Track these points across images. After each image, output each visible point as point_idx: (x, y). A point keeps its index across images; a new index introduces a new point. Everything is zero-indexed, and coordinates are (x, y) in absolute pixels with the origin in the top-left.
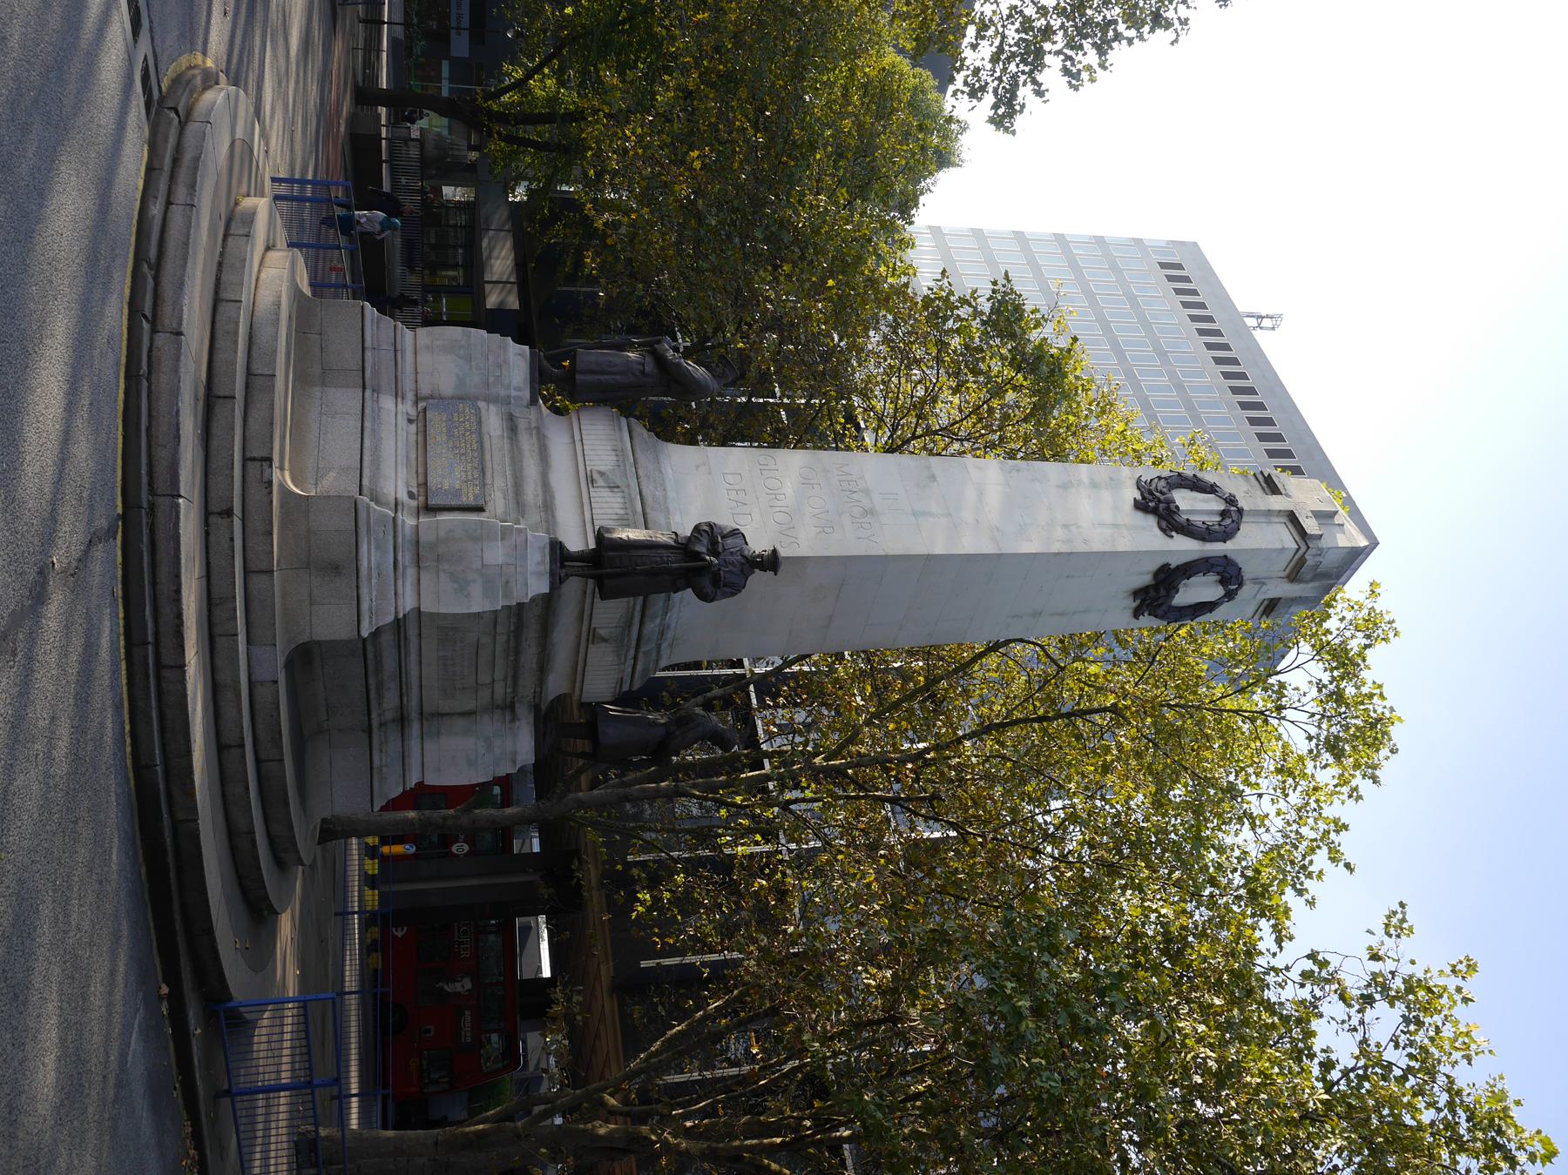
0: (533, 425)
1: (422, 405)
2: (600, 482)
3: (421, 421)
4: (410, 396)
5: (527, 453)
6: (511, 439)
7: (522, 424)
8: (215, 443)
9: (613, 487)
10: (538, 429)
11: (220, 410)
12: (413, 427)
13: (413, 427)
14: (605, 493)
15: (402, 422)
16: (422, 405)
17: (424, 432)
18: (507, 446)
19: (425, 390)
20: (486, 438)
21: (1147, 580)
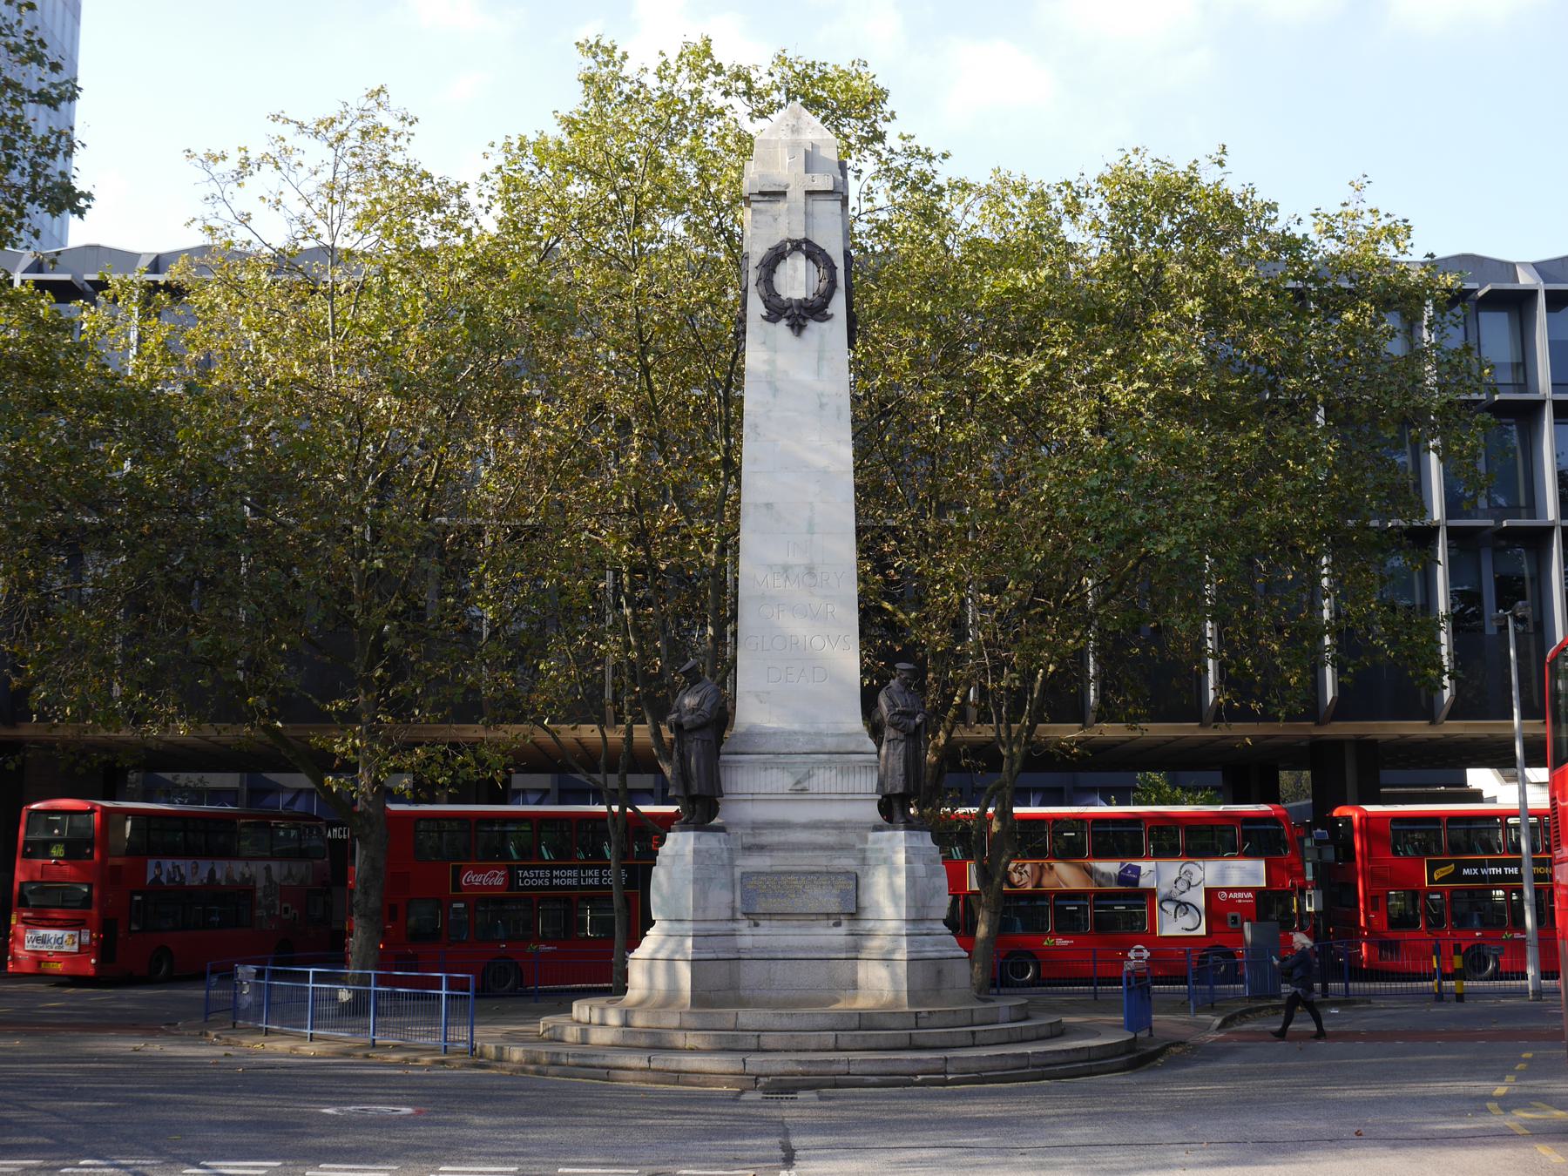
1: (739, 916)
2: (805, 784)
3: (754, 917)
4: (735, 925)
5: (782, 839)
6: (772, 850)
7: (749, 840)
8: (938, 1044)
9: (809, 776)
11: (920, 1041)
12: (762, 923)
13: (762, 923)
14: (814, 780)
15: (756, 931)
16: (739, 916)
17: (770, 915)
18: (781, 854)
19: (727, 914)
20: (775, 869)
21: (812, 325)
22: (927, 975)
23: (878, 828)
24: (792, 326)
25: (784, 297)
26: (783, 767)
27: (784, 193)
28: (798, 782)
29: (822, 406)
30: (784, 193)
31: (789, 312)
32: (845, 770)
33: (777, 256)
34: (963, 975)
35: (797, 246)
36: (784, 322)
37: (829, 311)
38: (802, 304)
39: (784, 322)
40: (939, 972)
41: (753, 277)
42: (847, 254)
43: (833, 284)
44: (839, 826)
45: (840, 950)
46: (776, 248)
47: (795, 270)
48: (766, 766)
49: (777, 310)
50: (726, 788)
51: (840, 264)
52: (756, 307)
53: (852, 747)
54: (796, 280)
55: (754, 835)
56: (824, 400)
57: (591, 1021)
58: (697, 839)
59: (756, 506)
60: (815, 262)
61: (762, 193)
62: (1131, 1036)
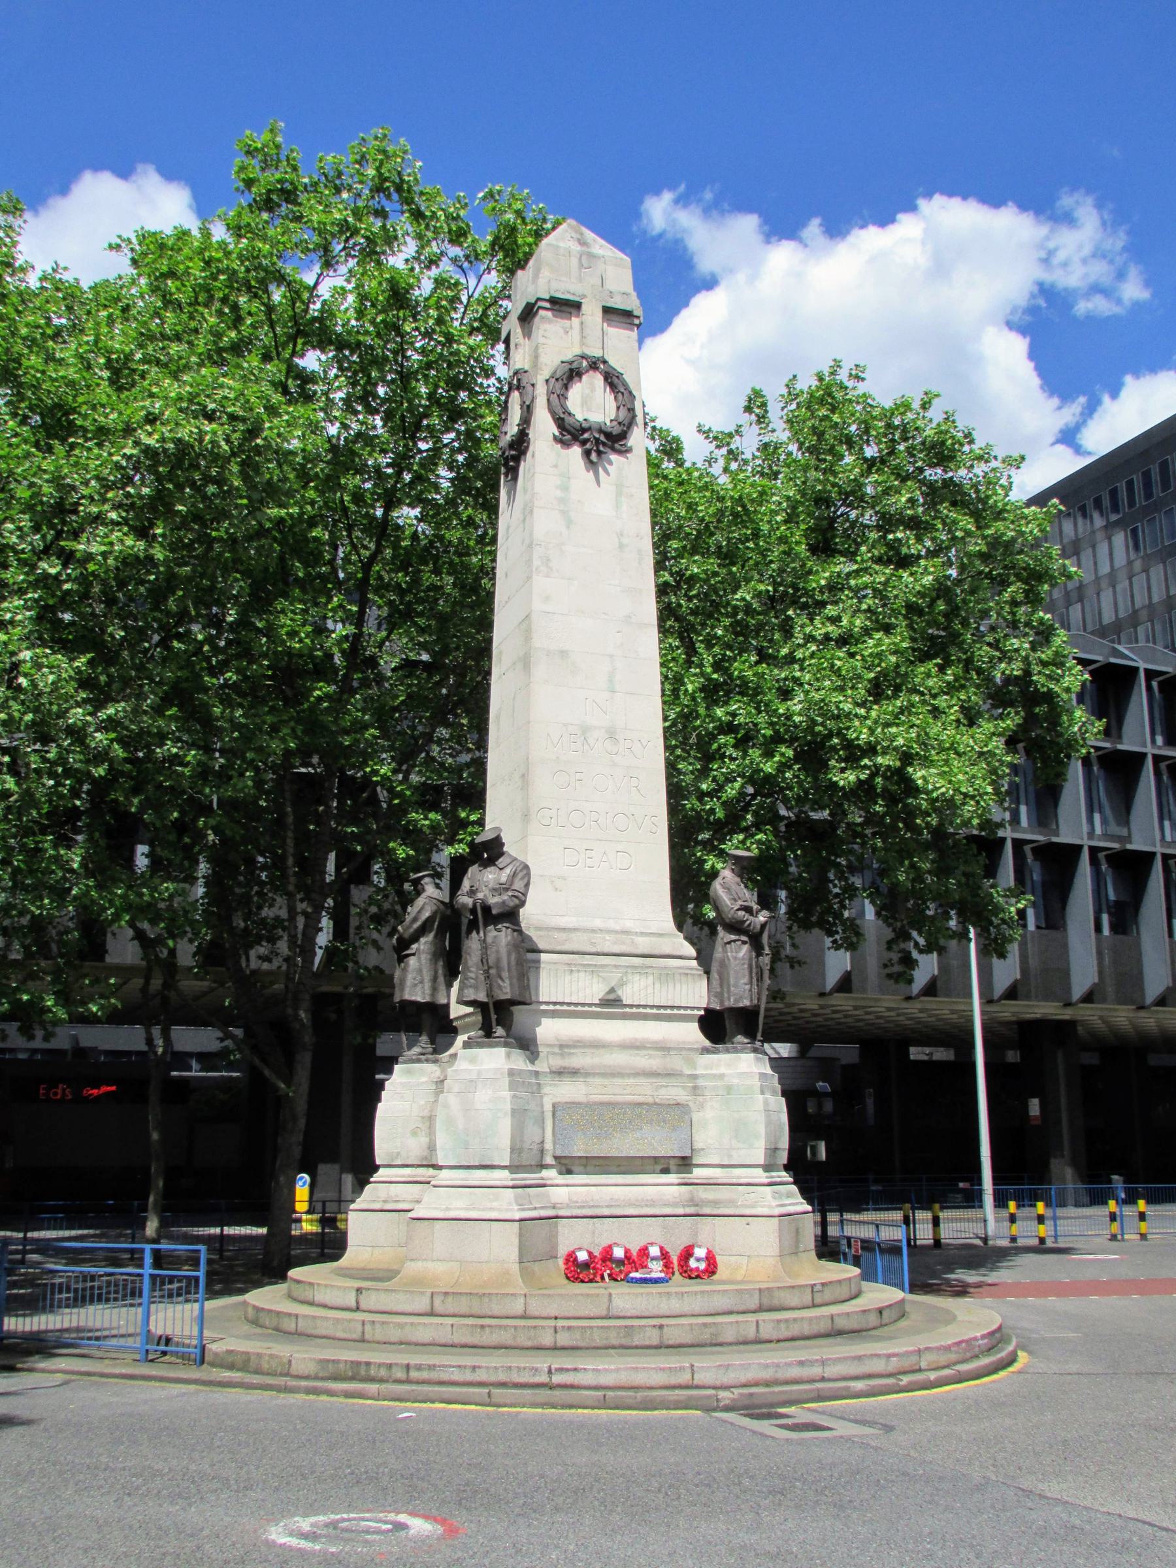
0: (557, 1050)
6: (587, 1075)
10: (561, 1046)
23: (705, 1051)
24: (587, 453)
25: (580, 417)
26: (593, 970)
28: (612, 990)
29: (621, 546)
31: (586, 436)
32: (666, 976)
33: (572, 374)
35: (594, 365)
36: (576, 450)
39: (576, 450)
44: (663, 1048)
47: (593, 390)
48: (571, 968)
49: (571, 432)
52: (543, 427)
53: (667, 950)
55: (562, 1055)
56: (625, 541)
58: (508, 1055)
61: (554, 301)
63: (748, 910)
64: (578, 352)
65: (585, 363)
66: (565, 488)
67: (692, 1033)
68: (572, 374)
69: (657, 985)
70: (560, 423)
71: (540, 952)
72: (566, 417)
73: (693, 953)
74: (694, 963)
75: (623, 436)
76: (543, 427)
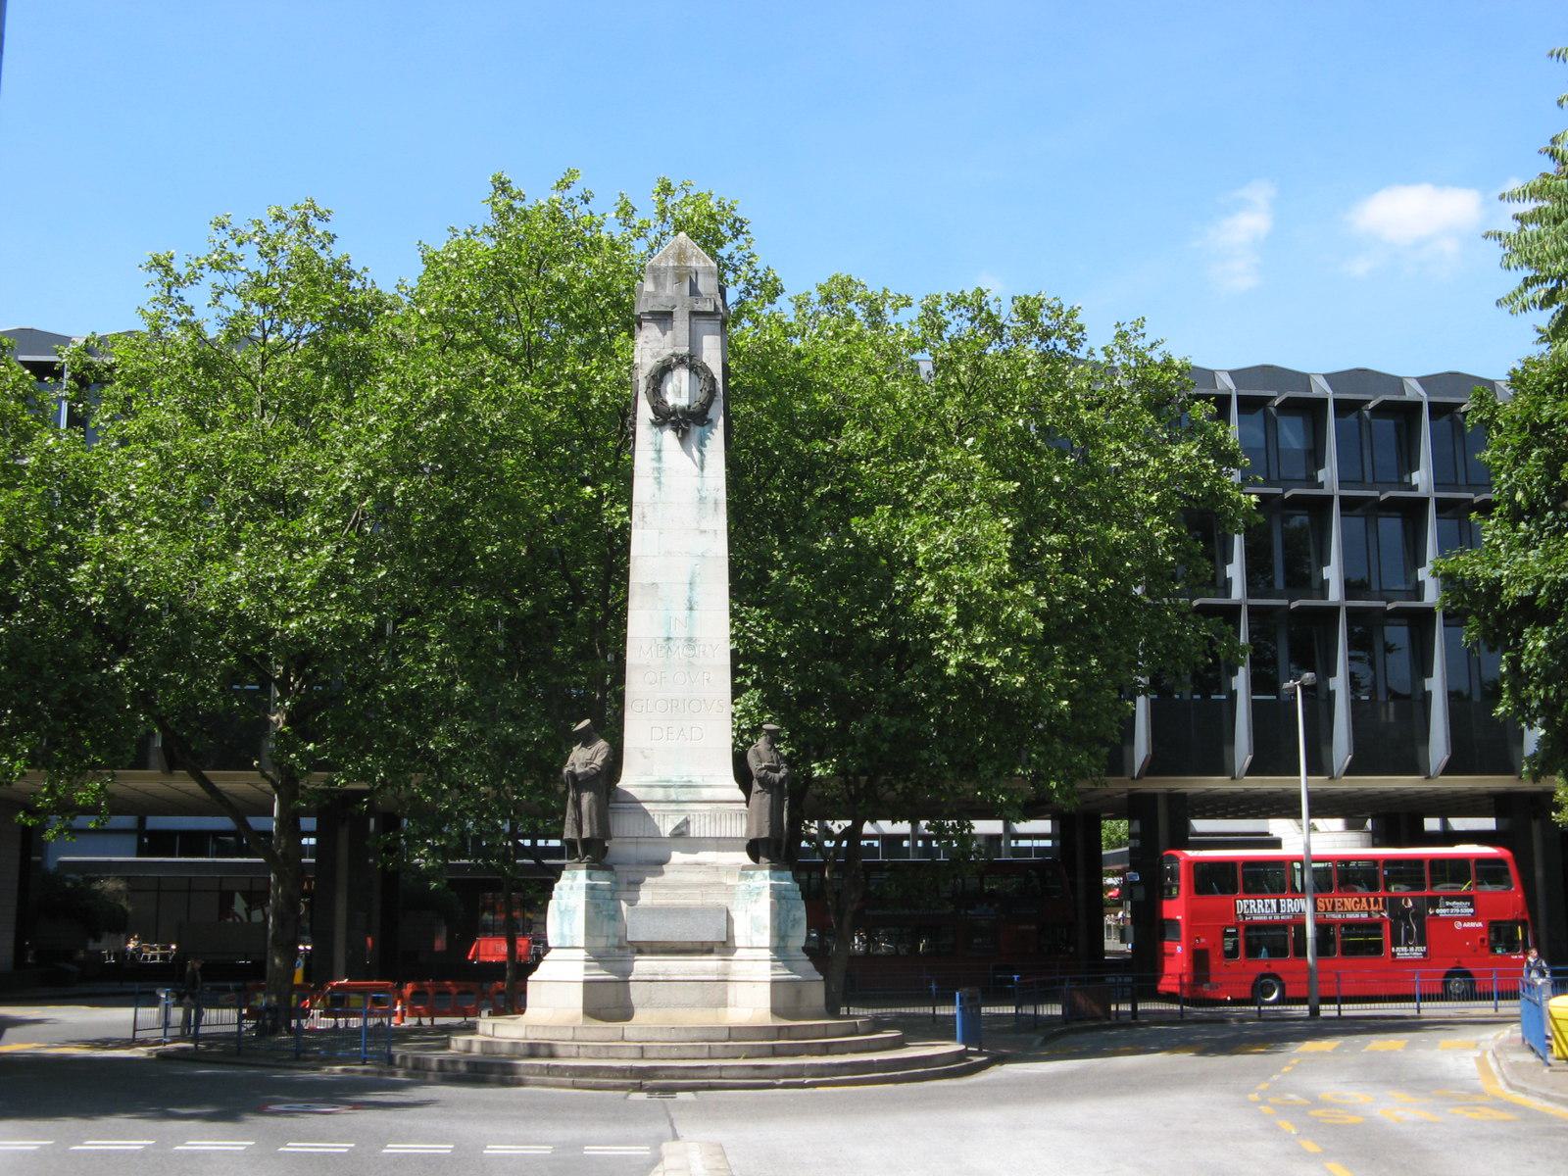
22: (785, 997)
27: (670, 314)
30: (670, 314)
33: (663, 371)
34: (817, 994)
35: (681, 361)
37: (709, 417)
38: (683, 411)
40: (799, 992)
41: (642, 385)
42: (725, 368)
43: (712, 394)
45: (712, 973)
46: (664, 361)
49: (664, 417)
50: (615, 831)
51: (719, 377)
52: (644, 411)
54: (679, 391)
57: (497, 1031)
59: (643, 586)
60: (696, 373)
62: (963, 1047)
63: (768, 768)
64: (671, 352)
65: (674, 360)
66: (659, 459)
67: (744, 858)
68: (663, 371)
69: (713, 824)
70: (655, 410)
71: (639, 802)
72: (660, 406)
73: (744, 798)
74: (743, 806)
75: (706, 412)
76: (644, 411)
